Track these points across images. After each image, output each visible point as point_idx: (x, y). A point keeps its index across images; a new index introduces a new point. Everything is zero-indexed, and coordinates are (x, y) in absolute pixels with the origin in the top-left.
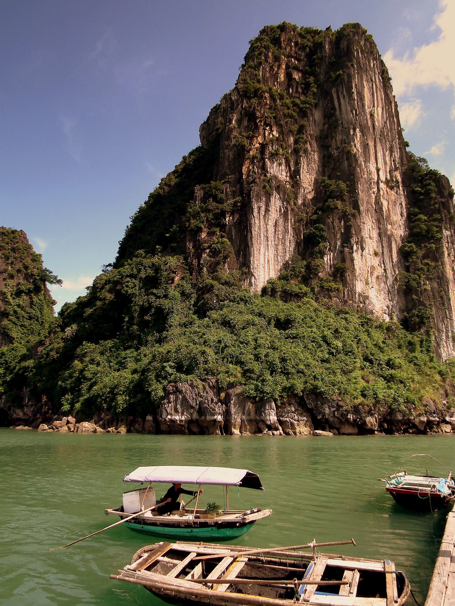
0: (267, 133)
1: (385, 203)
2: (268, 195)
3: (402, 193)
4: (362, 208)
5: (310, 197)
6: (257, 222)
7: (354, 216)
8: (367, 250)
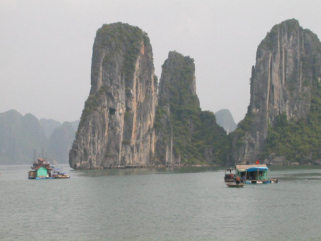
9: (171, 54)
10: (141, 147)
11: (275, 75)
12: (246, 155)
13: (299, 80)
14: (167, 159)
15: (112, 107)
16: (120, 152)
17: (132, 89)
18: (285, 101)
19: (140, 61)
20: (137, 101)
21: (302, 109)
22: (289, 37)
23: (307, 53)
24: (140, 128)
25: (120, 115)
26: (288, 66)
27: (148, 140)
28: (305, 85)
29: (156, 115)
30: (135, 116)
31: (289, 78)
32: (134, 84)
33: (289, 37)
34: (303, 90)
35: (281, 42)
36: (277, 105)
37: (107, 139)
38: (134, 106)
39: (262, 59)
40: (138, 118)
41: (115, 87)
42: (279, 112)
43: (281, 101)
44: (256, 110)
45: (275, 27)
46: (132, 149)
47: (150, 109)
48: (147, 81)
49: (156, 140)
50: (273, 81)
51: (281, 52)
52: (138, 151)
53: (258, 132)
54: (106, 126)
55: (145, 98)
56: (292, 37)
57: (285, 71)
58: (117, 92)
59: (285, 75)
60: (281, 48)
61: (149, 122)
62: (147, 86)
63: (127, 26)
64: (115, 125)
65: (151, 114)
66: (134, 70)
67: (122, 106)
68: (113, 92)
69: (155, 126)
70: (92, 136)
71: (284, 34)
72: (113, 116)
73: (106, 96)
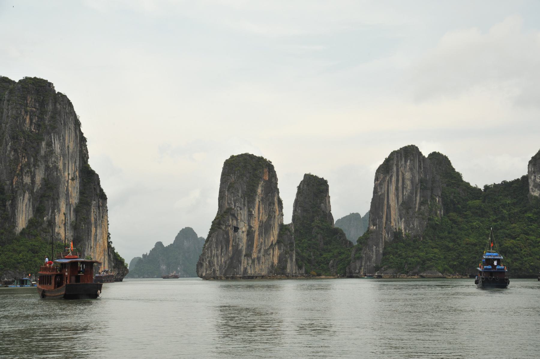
0: (23, 161)
1: (70, 189)
2: (25, 192)
3: (78, 181)
4: (60, 196)
5: (39, 188)
6: (19, 205)
7: (57, 199)
8: (61, 214)
9: (306, 175)
10: (263, 259)
11: (392, 196)
12: (363, 267)
14: (288, 271)
15: (236, 226)
16: (242, 264)
17: (254, 210)
18: (401, 219)
19: (262, 186)
20: (259, 221)
21: (417, 227)
22: (406, 162)
24: (261, 244)
25: (243, 232)
26: (406, 188)
27: (270, 254)
28: (422, 205)
29: (279, 232)
30: (257, 233)
31: (407, 198)
32: (256, 205)
34: (419, 209)
36: (394, 223)
37: (231, 253)
38: (256, 225)
39: (379, 182)
40: (260, 235)
41: (238, 209)
42: (396, 229)
43: (397, 219)
44: (373, 227)
45: (393, 154)
46: (253, 261)
47: (272, 227)
48: (270, 203)
49: (279, 254)
50: (390, 202)
52: (259, 263)
53: (375, 247)
54: (231, 242)
55: (268, 218)
56: (409, 161)
57: (403, 192)
58: (240, 213)
61: (272, 238)
62: (270, 207)
63: (252, 157)
64: (239, 241)
65: (274, 231)
66: (256, 195)
67: (245, 225)
68: (236, 213)
69: (278, 242)
70: (215, 250)
71: (401, 160)
72: (236, 233)
73: (230, 217)
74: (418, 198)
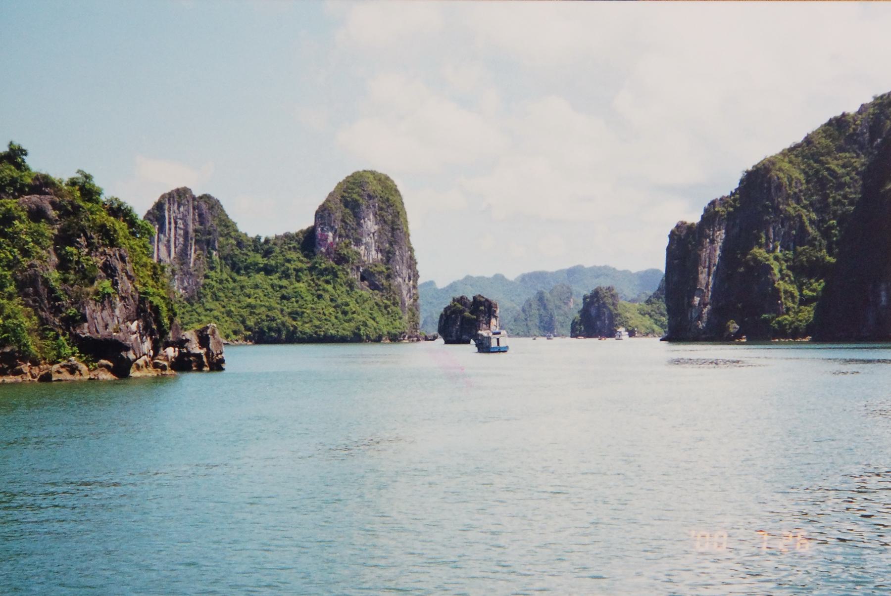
11: (163, 249)
13: (190, 255)
23: (201, 223)
33: (179, 207)
35: (169, 212)
45: (163, 197)
51: (170, 223)
57: (175, 243)
59: (176, 247)
60: (170, 218)
74: (193, 251)
